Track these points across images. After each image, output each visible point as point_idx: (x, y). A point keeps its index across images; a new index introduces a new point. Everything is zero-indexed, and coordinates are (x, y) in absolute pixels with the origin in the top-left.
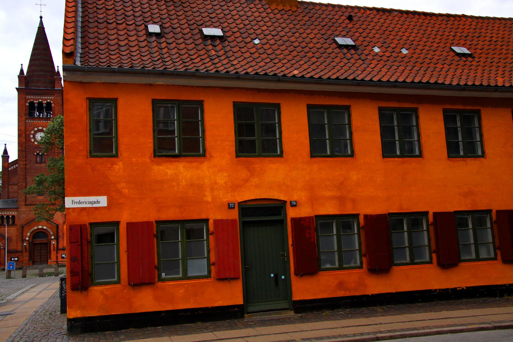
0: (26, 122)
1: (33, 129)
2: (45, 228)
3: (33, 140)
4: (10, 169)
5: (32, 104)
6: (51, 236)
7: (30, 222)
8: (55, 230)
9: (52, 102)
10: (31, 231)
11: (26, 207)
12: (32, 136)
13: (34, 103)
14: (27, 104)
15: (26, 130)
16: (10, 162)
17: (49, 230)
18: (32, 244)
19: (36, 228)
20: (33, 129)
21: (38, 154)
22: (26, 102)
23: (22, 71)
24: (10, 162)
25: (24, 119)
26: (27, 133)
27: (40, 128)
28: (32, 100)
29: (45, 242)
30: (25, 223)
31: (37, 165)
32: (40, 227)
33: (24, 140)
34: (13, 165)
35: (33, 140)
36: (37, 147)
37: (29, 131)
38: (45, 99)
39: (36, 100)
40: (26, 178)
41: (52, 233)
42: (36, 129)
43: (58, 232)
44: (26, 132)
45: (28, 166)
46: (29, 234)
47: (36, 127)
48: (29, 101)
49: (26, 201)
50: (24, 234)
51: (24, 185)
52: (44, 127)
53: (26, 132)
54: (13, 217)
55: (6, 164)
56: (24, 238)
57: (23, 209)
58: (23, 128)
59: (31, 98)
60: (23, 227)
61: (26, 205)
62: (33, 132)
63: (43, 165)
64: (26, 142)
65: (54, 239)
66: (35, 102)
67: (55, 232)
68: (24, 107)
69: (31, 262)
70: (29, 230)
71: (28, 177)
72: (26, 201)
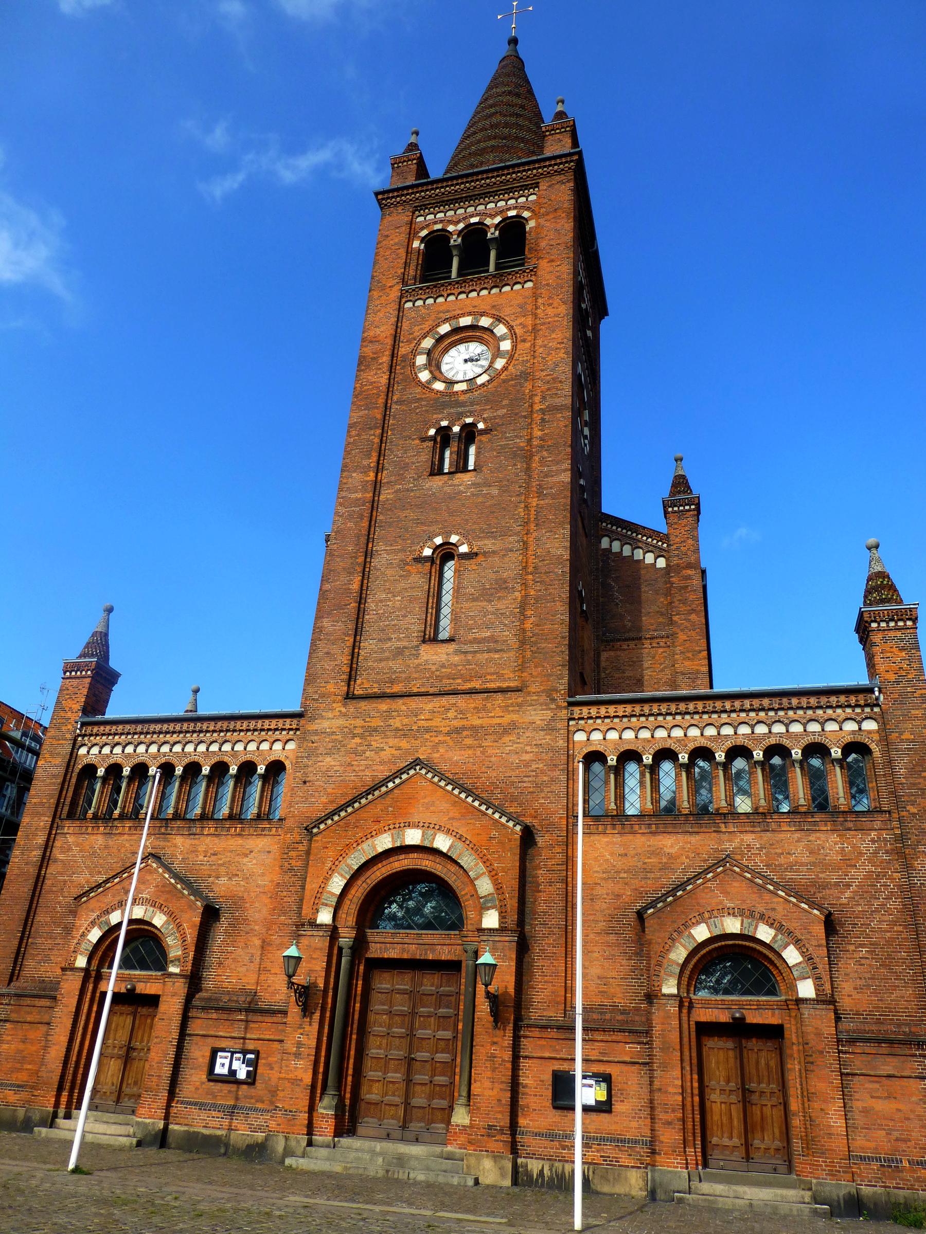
0: (400, 309)
2: (442, 843)
3: (424, 376)
6: (482, 909)
7: (363, 800)
8: (510, 860)
9: (526, 214)
11: (352, 707)
15: (396, 338)
17: (467, 860)
22: (412, 235)
26: (404, 350)
29: (445, 954)
33: (384, 380)
35: (424, 376)
37: (409, 341)
40: (368, 554)
41: (485, 886)
42: (445, 329)
45: (386, 495)
47: (446, 320)
48: (424, 233)
49: (351, 678)
50: (311, 886)
51: (355, 586)
54: (276, 768)
56: (306, 911)
64: (390, 386)
65: (502, 929)
67: (511, 881)
68: (402, 252)
69: (326, 1109)
71: (380, 547)
72: (351, 678)
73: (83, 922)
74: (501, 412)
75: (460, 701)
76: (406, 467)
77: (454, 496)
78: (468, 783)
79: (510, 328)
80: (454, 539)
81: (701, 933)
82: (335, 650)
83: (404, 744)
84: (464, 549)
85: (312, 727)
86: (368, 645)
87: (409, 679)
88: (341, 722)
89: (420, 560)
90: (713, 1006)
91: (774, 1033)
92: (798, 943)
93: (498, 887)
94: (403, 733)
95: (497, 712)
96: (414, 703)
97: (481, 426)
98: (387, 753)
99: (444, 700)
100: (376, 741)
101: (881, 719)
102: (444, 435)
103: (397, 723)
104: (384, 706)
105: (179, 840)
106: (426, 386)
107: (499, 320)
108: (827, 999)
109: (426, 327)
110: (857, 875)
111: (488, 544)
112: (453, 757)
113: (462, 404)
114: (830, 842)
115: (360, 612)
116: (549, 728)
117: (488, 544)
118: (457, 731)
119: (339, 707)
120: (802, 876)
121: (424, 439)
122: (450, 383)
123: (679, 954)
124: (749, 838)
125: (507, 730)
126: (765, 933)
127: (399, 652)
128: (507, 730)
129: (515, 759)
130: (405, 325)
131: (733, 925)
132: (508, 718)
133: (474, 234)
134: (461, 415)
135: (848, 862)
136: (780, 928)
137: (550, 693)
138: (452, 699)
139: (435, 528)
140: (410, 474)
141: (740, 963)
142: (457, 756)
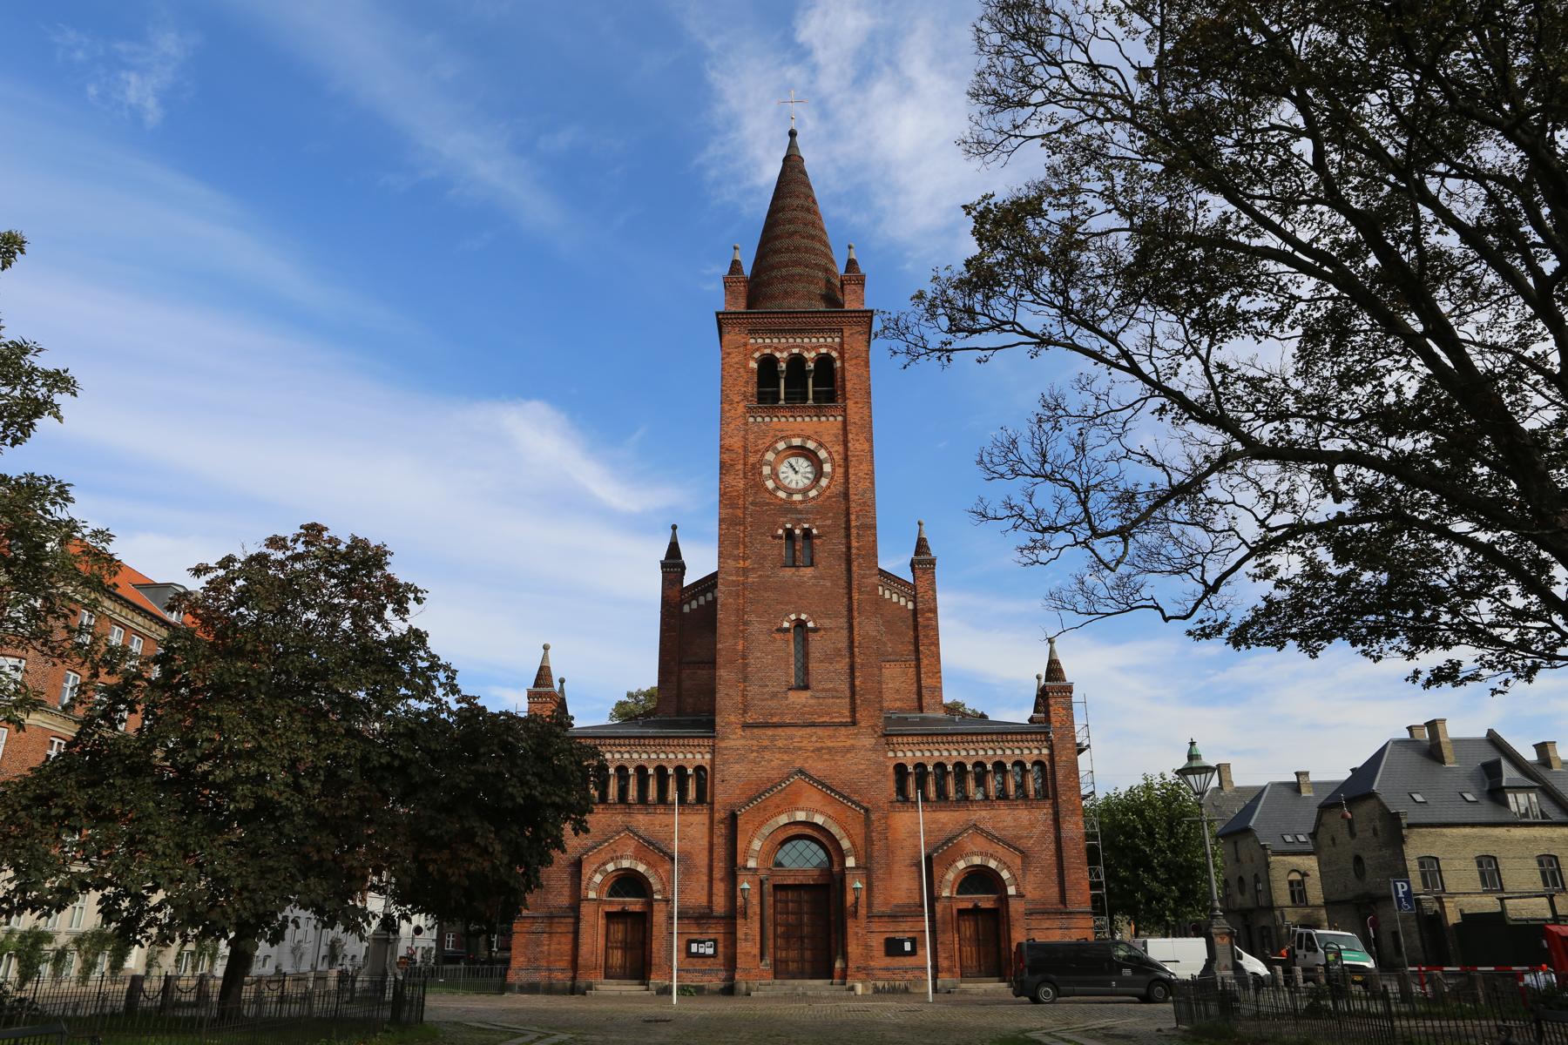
0: (746, 424)
2: (819, 819)
3: (770, 484)
4: (686, 609)
5: (768, 363)
7: (762, 794)
10: (766, 830)
11: (748, 732)
12: (766, 470)
13: (777, 360)
14: (753, 365)
15: (745, 448)
16: (687, 582)
19: (783, 819)
20: (771, 447)
22: (748, 356)
23: (735, 266)
24: (687, 582)
28: (768, 351)
30: (743, 799)
31: (789, 572)
32: (801, 816)
34: (695, 597)
36: (788, 508)
37: (756, 452)
38: (812, 347)
39: (783, 349)
41: (846, 844)
43: (869, 841)
44: (745, 457)
46: (757, 845)
47: (782, 438)
48: (757, 355)
50: (741, 846)
51: (740, 647)
52: (809, 438)
53: (745, 457)
55: (674, 592)
56: (740, 860)
57: (733, 739)
59: (765, 344)
61: (746, 726)
62: (770, 456)
63: (809, 571)
66: (778, 355)
67: (859, 841)
70: (762, 824)
73: (586, 871)
74: (829, 522)
75: (819, 731)
76: (765, 557)
77: (800, 584)
78: (828, 782)
79: (830, 453)
80: (803, 617)
81: (961, 865)
82: (731, 692)
83: (785, 757)
84: (810, 624)
85: (723, 745)
86: (753, 689)
87: (782, 714)
88: (742, 742)
89: (781, 630)
90: (966, 902)
92: (1008, 868)
93: (853, 844)
94: (786, 750)
95: (843, 738)
96: (789, 731)
97: (815, 531)
98: (775, 763)
99: (808, 730)
100: (767, 755)
101: (1051, 748)
102: (790, 534)
103: (780, 743)
104: (770, 732)
105: (640, 817)
106: (772, 493)
107: (821, 445)
108: (1020, 895)
109: (768, 441)
110: (1037, 832)
111: (827, 623)
112: (817, 767)
113: (800, 512)
114: (1024, 815)
115: (745, 666)
116: (874, 750)
117: (827, 623)
118: (819, 749)
119: (739, 732)
120: (1010, 833)
121: (775, 537)
122: (790, 493)
123: (950, 876)
124: (984, 813)
125: (851, 749)
126: (993, 864)
127: (774, 695)
128: (851, 749)
129: (854, 768)
130: (751, 437)
131: (977, 860)
132: (849, 743)
133: (797, 362)
134: (799, 521)
135: (1032, 825)
136: (1000, 861)
137: (873, 727)
138: (814, 730)
139: (790, 607)
140: (768, 564)
141: (980, 879)
142: (820, 765)
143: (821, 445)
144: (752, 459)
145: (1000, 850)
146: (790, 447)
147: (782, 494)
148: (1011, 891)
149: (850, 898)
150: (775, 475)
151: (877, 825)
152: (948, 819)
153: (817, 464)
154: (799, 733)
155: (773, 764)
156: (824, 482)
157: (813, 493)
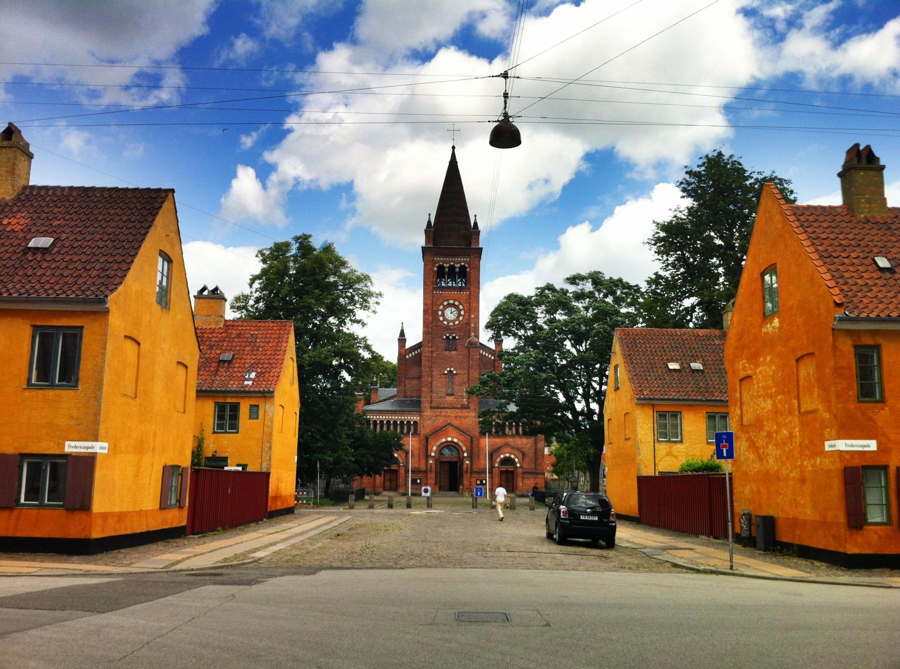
1: (442, 304)
2: (455, 440)
3: (441, 319)
5: (441, 268)
7: (437, 432)
8: (469, 444)
10: (438, 444)
12: (440, 313)
13: (444, 267)
14: (435, 269)
17: (460, 444)
18: (441, 462)
19: (444, 440)
20: (442, 304)
21: (448, 338)
23: (429, 222)
25: (431, 288)
27: (451, 302)
31: (447, 353)
32: (449, 439)
34: (411, 352)
36: (447, 328)
38: (458, 262)
39: (447, 263)
41: (464, 449)
43: (472, 448)
46: (435, 448)
54: (415, 422)
57: (428, 413)
58: (429, 302)
59: (440, 260)
60: (427, 439)
61: (431, 408)
63: (454, 352)
81: (502, 456)
86: (434, 395)
90: (504, 468)
91: (512, 472)
95: (465, 413)
102: (448, 338)
107: (460, 303)
108: (521, 467)
111: (460, 372)
112: (456, 422)
114: (524, 440)
117: (460, 372)
120: (519, 446)
123: (498, 460)
126: (513, 456)
127: (441, 397)
131: (507, 455)
133: (452, 268)
135: (527, 444)
141: (507, 461)
143: (460, 303)
144: (435, 308)
145: (515, 452)
146: (449, 304)
147: (445, 323)
148: (518, 465)
149: (465, 466)
150: (443, 315)
151: (475, 443)
152: (499, 441)
153: (459, 311)
154: (449, 411)
155: (440, 421)
156: (461, 318)
157: (457, 323)
